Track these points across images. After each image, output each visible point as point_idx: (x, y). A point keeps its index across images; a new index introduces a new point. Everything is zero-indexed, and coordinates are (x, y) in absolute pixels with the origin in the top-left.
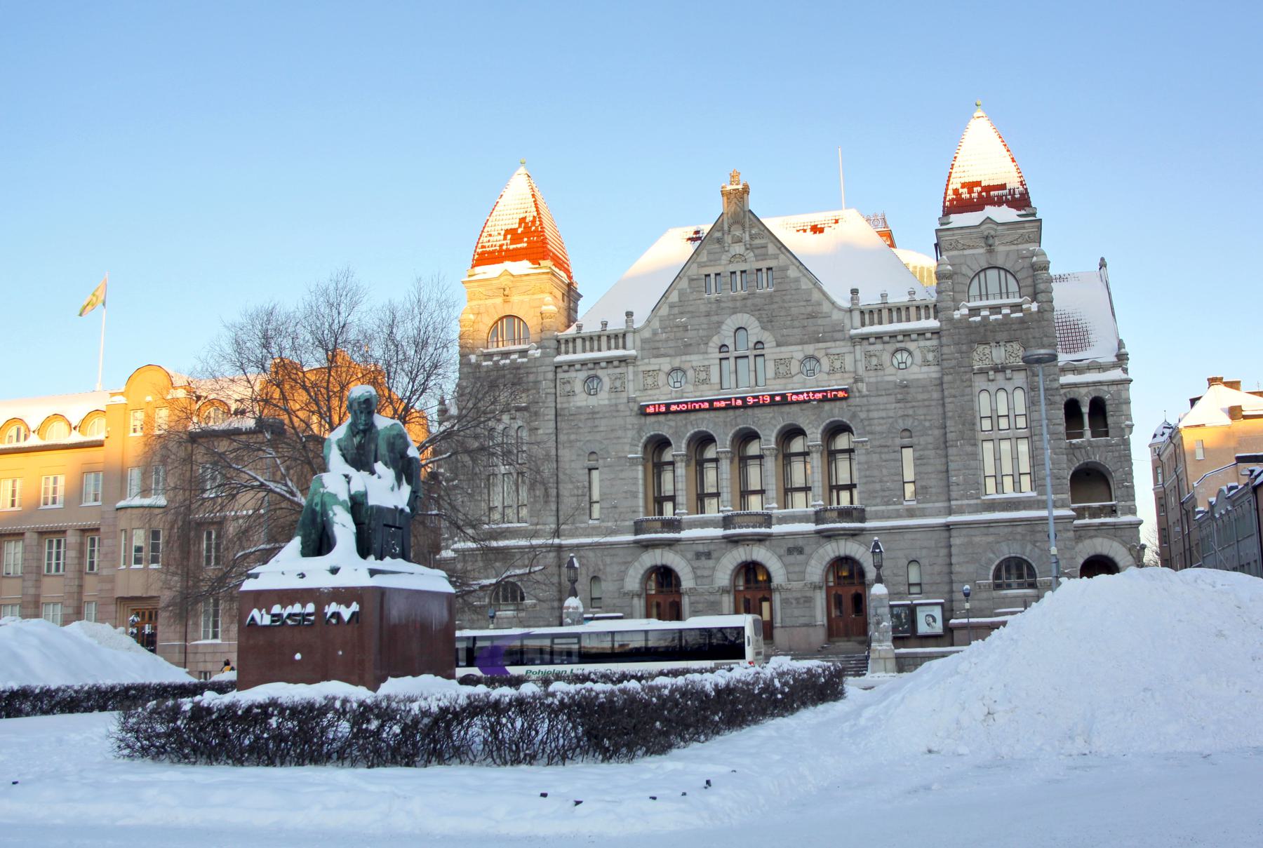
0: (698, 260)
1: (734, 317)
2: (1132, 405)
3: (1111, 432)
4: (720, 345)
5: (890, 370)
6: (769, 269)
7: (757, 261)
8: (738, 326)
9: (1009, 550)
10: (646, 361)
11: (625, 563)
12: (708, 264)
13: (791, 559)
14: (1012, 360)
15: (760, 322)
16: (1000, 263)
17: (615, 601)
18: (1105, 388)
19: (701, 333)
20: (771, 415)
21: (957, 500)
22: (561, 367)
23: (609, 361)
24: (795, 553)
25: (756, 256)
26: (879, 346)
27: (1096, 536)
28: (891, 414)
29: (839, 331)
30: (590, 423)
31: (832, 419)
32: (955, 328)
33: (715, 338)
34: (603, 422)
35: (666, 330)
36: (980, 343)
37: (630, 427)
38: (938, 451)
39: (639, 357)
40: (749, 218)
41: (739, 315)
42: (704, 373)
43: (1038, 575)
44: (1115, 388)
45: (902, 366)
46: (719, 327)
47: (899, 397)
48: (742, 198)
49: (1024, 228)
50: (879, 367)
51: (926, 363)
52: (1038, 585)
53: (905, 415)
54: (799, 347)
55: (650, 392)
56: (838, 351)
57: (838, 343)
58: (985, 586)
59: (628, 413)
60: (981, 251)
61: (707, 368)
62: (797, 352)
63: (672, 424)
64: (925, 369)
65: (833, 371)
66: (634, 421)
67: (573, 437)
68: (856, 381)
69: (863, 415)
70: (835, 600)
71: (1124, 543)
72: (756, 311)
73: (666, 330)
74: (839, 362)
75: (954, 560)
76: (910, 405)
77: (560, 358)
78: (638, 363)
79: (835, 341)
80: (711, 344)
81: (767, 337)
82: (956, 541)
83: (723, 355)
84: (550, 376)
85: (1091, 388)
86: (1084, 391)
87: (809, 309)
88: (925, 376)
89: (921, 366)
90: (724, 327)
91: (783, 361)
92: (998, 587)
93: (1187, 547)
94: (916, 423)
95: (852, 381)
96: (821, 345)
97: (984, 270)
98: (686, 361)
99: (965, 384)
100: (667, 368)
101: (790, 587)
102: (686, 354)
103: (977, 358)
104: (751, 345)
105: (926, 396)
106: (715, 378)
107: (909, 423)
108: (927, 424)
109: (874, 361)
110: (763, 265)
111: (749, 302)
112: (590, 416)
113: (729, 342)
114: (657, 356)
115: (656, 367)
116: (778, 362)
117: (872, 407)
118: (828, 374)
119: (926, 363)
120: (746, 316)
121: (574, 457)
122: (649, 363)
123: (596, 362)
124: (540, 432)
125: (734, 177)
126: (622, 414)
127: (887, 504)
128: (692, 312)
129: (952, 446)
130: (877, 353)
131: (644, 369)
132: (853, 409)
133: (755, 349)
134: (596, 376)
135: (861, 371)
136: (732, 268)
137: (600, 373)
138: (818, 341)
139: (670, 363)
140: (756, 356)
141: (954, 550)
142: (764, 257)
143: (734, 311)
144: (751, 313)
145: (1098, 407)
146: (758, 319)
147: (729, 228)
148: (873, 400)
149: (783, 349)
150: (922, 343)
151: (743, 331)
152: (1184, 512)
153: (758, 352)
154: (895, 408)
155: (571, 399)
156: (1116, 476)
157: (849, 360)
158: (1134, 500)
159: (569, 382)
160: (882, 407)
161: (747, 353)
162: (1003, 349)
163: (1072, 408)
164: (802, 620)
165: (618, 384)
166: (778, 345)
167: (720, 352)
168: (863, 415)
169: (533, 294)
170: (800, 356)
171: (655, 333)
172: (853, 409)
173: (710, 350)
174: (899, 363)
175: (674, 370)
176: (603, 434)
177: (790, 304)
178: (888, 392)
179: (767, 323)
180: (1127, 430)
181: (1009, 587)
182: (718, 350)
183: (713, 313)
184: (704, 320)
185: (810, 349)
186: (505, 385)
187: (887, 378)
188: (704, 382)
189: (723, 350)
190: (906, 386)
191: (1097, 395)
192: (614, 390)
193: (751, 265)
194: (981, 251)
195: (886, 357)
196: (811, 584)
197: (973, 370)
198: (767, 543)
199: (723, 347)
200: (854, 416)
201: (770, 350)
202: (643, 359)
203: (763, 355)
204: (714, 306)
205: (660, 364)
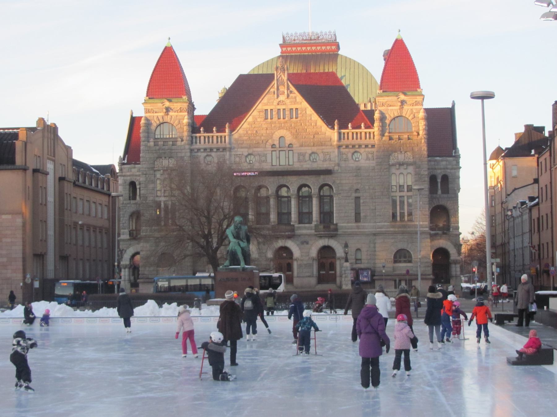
0: (262, 102)
1: (279, 131)
2: (461, 179)
3: (450, 192)
4: (272, 144)
6: (297, 109)
8: (281, 136)
9: (400, 246)
10: (236, 150)
14: (407, 160)
16: (404, 115)
18: (449, 171)
20: (296, 179)
21: (379, 223)
22: (194, 150)
24: (305, 243)
26: (347, 150)
27: (441, 239)
29: (329, 141)
31: (324, 183)
33: (270, 141)
35: (246, 135)
39: (233, 148)
40: (288, 84)
41: (282, 131)
42: (264, 157)
43: (413, 257)
44: (453, 171)
45: (357, 160)
47: (354, 174)
48: (285, 72)
49: (416, 98)
52: (413, 262)
53: (357, 183)
54: (310, 148)
57: (328, 147)
58: (390, 261)
64: (368, 162)
69: (338, 182)
70: (321, 266)
71: (452, 242)
73: (246, 135)
74: (328, 156)
75: (377, 249)
76: (360, 178)
78: (232, 150)
79: (327, 146)
80: (268, 144)
83: (273, 149)
84: (188, 154)
85: (442, 170)
86: (439, 171)
87: (315, 130)
89: (366, 160)
91: (302, 154)
92: (395, 262)
93: (503, 230)
94: (362, 187)
97: (397, 117)
98: (255, 151)
101: (302, 259)
102: (255, 148)
106: (269, 160)
107: (359, 186)
108: (367, 187)
109: (344, 156)
110: (294, 107)
113: (276, 143)
114: (242, 148)
115: (241, 153)
119: (368, 159)
120: (285, 131)
122: (237, 151)
123: (211, 150)
127: (348, 223)
130: (346, 153)
131: (235, 154)
132: (334, 179)
133: (289, 147)
134: (210, 155)
136: (279, 107)
140: (289, 151)
141: (377, 245)
142: (295, 102)
143: (280, 128)
145: (445, 178)
149: (302, 148)
150: (367, 150)
151: (282, 138)
152: (503, 209)
154: (353, 179)
156: (451, 212)
158: (458, 223)
159: (197, 158)
161: (285, 149)
162: (403, 155)
163: (433, 179)
164: (307, 274)
167: (272, 148)
170: (310, 152)
172: (334, 179)
173: (267, 146)
174: (356, 158)
175: (249, 154)
178: (350, 172)
180: (457, 191)
181: (400, 262)
182: (271, 147)
184: (265, 132)
186: (165, 158)
187: (352, 165)
188: (263, 162)
189: (273, 146)
191: (443, 173)
194: (398, 108)
195: (350, 155)
196: (312, 258)
197: (390, 164)
198: (292, 239)
200: (334, 182)
203: (293, 150)
205: (243, 152)
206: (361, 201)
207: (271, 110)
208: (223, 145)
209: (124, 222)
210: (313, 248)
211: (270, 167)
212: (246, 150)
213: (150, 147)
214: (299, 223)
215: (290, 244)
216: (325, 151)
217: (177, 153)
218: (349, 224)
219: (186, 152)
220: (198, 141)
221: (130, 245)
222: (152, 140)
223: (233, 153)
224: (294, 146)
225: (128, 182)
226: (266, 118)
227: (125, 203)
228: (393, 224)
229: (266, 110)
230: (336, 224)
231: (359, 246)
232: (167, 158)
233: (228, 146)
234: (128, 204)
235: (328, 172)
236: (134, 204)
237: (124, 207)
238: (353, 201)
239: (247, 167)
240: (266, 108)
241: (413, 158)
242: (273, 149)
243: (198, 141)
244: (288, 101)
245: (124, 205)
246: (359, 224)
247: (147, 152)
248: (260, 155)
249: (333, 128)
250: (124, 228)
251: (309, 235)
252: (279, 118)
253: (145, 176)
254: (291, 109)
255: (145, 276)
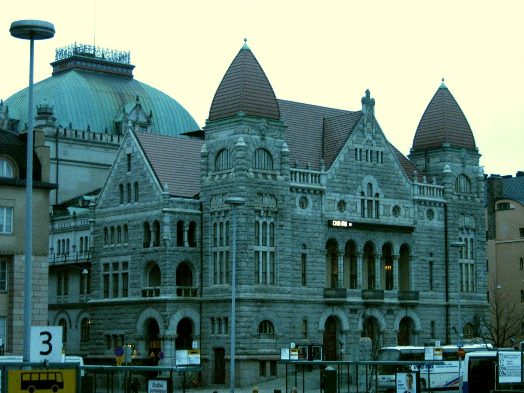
1: (367, 176)
5: (426, 220)
6: (382, 152)
7: (377, 146)
10: (329, 193)
11: (320, 313)
12: (356, 142)
13: (388, 317)
15: (378, 182)
16: (467, 173)
17: (315, 335)
19: (354, 182)
20: (381, 236)
23: (315, 191)
25: (377, 143)
28: (427, 244)
30: (303, 226)
32: (453, 204)
33: (359, 187)
34: (310, 226)
36: (463, 214)
37: (321, 231)
38: (442, 266)
41: (370, 176)
46: (361, 181)
50: (422, 218)
51: (439, 219)
55: (330, 213)
56: (407, 205)
59: (321, 223)
60: (459, 165)
61: (356, 203)
62: (392, 203)
63: (341, 233)
64: (439, 222)
65: (405, 217)
66: (323, 228)
67: (295, 233)
68: (415, 223)
69: (417, 242)
72: (376, 175)
77: (293, 184)
81: (379, 191)
82: (452, 312)
83: (362, 197)
87: (397, 180)
88: (439, 226)
90: (363, 181)
95: (412, 223)
96: (401, 201)
99: (456, 233)
100: (338, 200)
102: (347, 193)
103: (459, 221)
104: (374, 194)
105: (438, 236)
107: (433, 250)
110: (380, 149)
111: (374, 169)
112: (303, 222)
113: (365, 190)
115: (334, 198)
116: (385, 206)
117: (420, 239)
118: (404, 217)
121: (295, 246)
122: (330, 195)
123: (309, 190)
124: (284, 228)
125: (368, 92)
126: (318, 223)
128: (350, 169)
129: (451, 265)
132: (413, 238)
134: (305, 198)
135: (416, 219)
136: (367, 148)
137: (309, 197)
138: (401, 198)
139: (340, 197)
143: (367, 173)
144: (374, 175)
146: (377, 180)
147: (367, 122)
148: (420, 235)
153: (376, 199)
155: (294, 209)
157: (412, 211)
160: (423, 239)
165: (316, 204)
166: (385, 197)
168: (417, 242)
169: (277, 138)
171: (333, 178)
176: (309, 234)
177: (391, 175)
179: (382, 183)
183: (358, 172)
184: (354, 175)
185: (397, 202)
188: (355, 211)
190: (432, 230)
192: (314, 208)
193: (375, 149)
199: (362, 193)
201: (382, 200)
202: (328, 192)
204: (359, 167)
205: (335, 197)
206: (435, 266)
207: (361, 150)
208: (317, 186)
209: (171, 276)
210: (397, 319)
211: (359, 218)
212: (338, 195)
213: (250, 179)
214: (387, 289)
215: (376, 313)
216: (406, 205)
217: (278, 189)
218: (425, 293)
219: (287, 191)
220: (293, 178)
221: (178, 307)
222: (250, 170)
223: (327, 197)
224: (380, 196)
225: (176, 222)
226: (356, 159)
227: (172, 249)
228: (462, 294)
229: (356, 149)
230: (417, 293)
231: (433, 318)
232: (268, 195)
233: (324, 188)
234: (176, 251)
235: (409, 230)
236: (183, 252)
237: (172, 254)
238: (428, 266)
239: (339, 217)
240: (356, 146)
241: (476, 222)
242: (362, 197)
243: (293, 178)
244: (374, 142)
245: (171, 252)
246: (432, 293)
247: (248, 184)
248: (351, 204)
249: (413, 181)
250: (171, 284)
251: (358, 304)
252: (367, 161)
253: (245, 216)
254: (378, 152)
255: (247, 351)
